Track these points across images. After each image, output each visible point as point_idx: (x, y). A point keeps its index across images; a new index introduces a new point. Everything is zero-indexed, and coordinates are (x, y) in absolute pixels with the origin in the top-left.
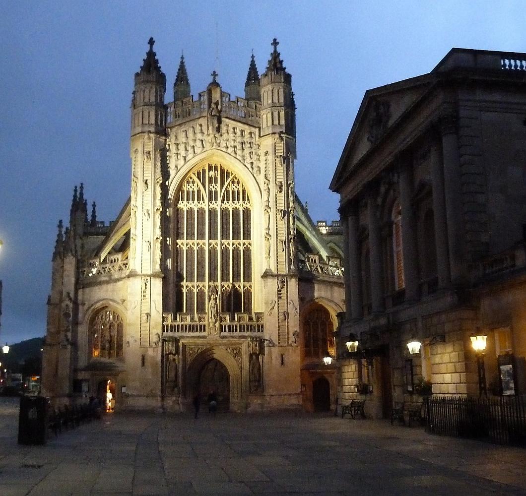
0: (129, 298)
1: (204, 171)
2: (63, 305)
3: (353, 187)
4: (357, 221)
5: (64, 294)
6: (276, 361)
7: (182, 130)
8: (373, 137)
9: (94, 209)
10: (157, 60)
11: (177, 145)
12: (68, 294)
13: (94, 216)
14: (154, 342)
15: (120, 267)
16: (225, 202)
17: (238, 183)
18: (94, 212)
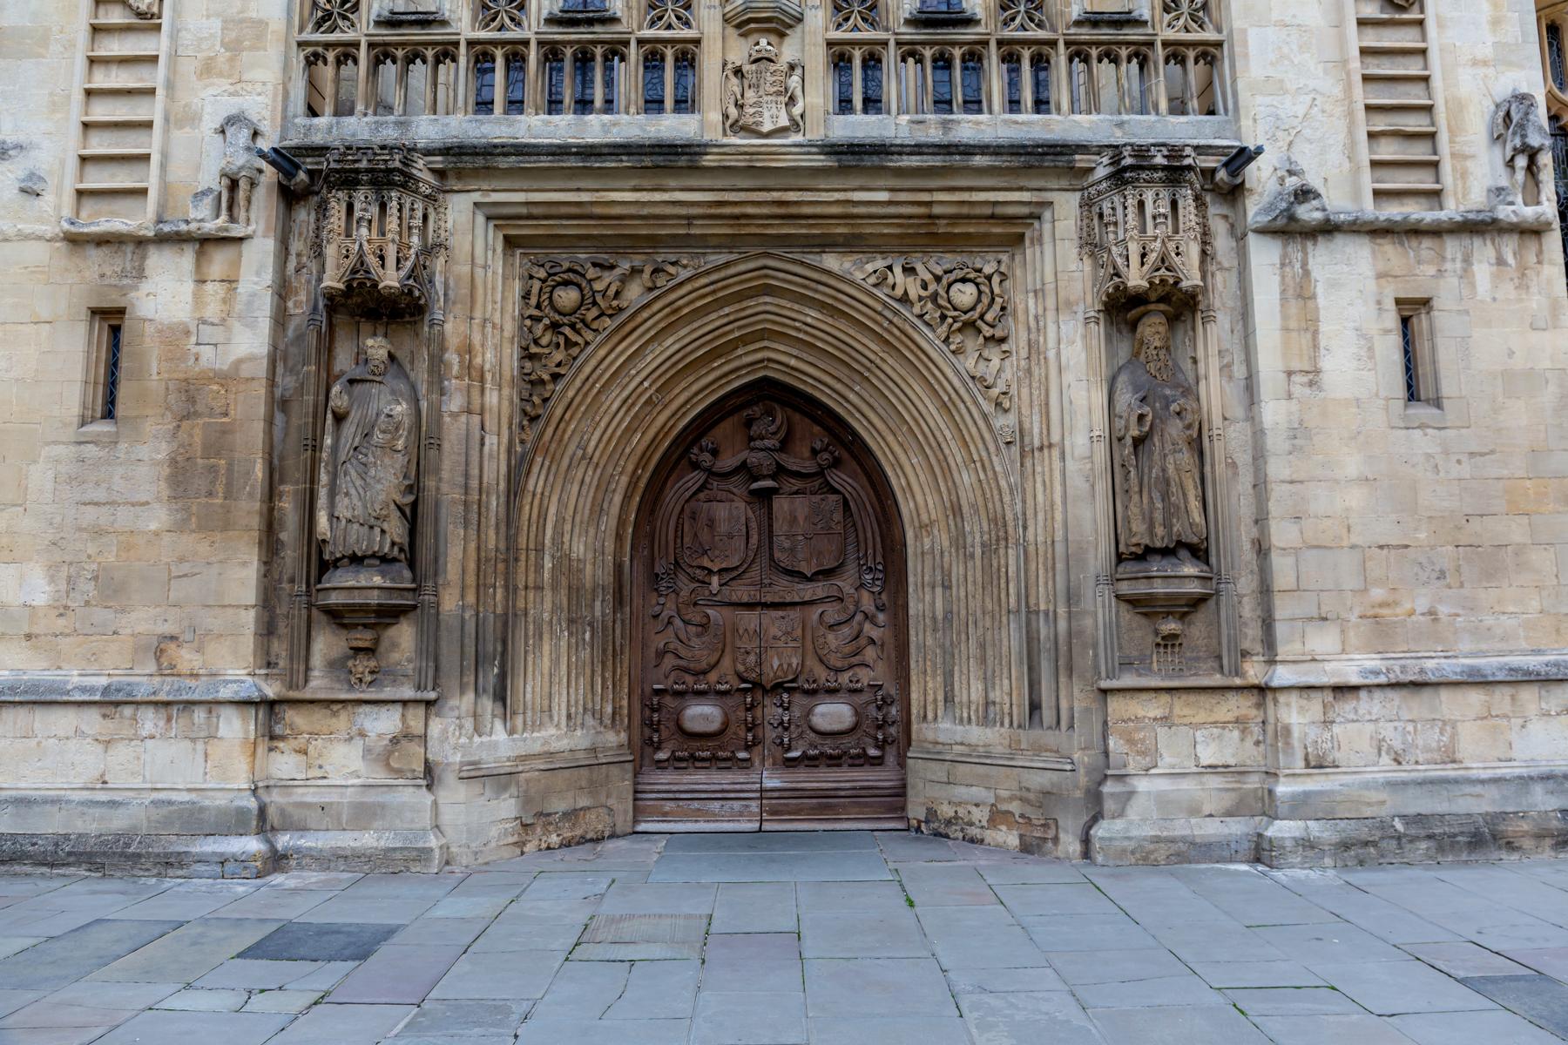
14: (199, 196)
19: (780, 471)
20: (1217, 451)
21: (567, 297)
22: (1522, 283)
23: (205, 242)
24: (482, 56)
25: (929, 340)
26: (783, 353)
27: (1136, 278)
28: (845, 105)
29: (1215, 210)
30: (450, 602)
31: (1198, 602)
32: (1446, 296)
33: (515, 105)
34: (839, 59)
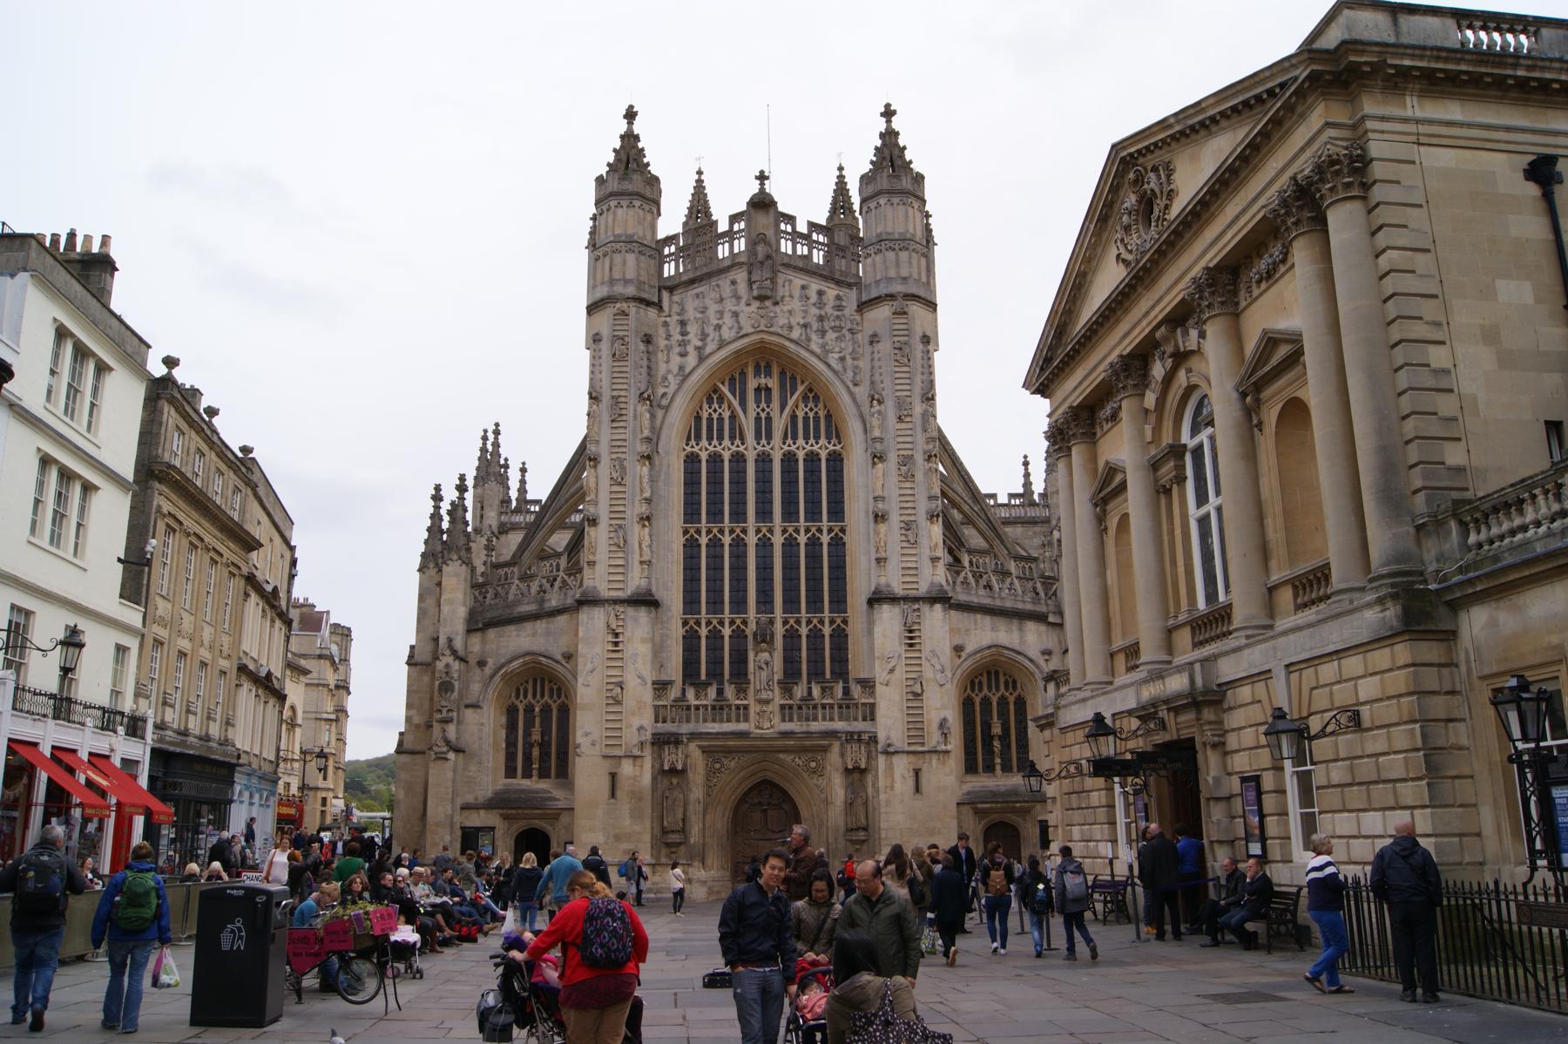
0: (582, 649)
1: (743, 374)
2: (440, 665)
3: (1078, 384)
4: (1093, 458)
5: (442, 641)
6: (903, 784)
7: (695, 291)
8: (1131, 252)
9: (523, 476)
10: (643, 150)
11: (683, 323)
12: (450, 640)
13: (522, 490)
15: (564, 581)
16: (789, 441)
17: (816, 399)
18: (523, 482)
19: (769, 804)
20: (870, 805)
21: (718, 766)
22: (944, 764)
23: (635, 757)
24: (697, 708)
25: (805, 775)
26: (769, 774)
27: (850, 767)
28: (783, 720)
29: (872, 745)
30: (692, 841)
31: (864, 841)
32: (925, 768)
33: (705, 721)
34: (782, 707)
